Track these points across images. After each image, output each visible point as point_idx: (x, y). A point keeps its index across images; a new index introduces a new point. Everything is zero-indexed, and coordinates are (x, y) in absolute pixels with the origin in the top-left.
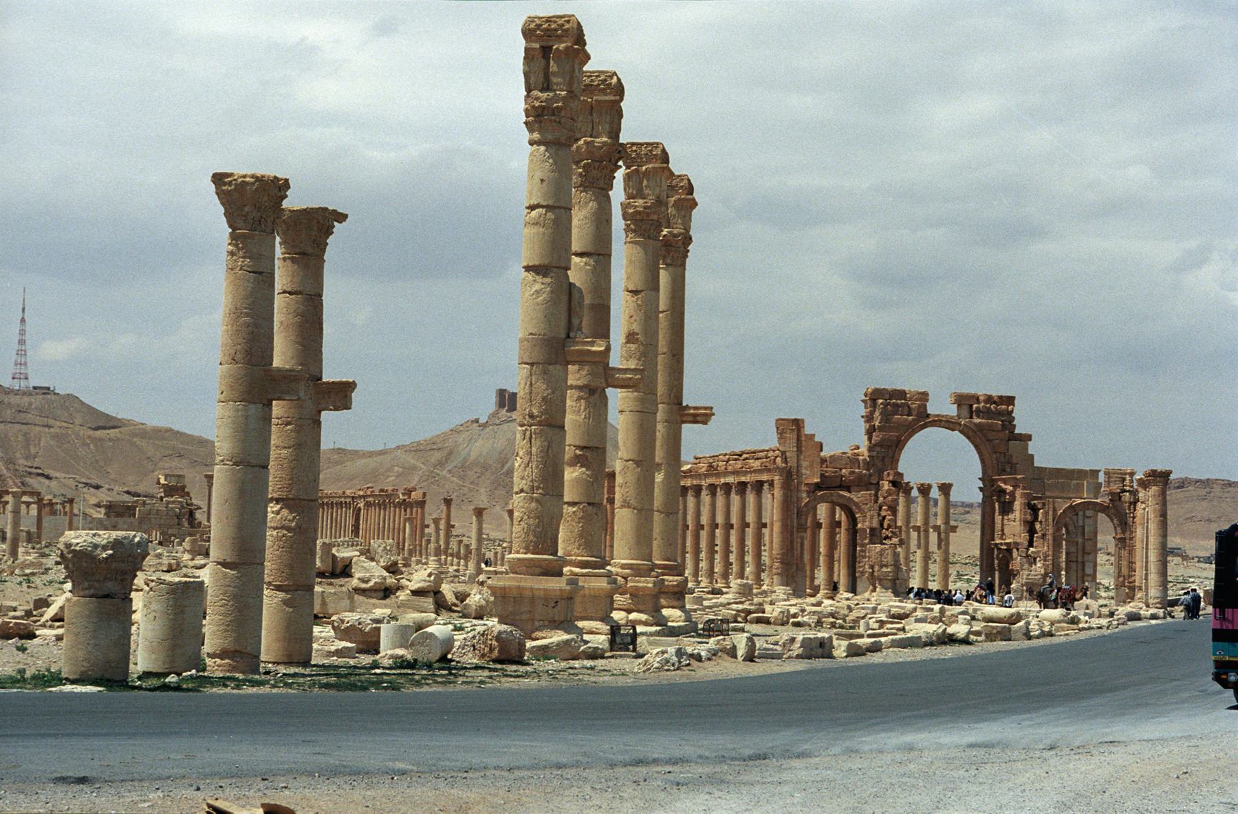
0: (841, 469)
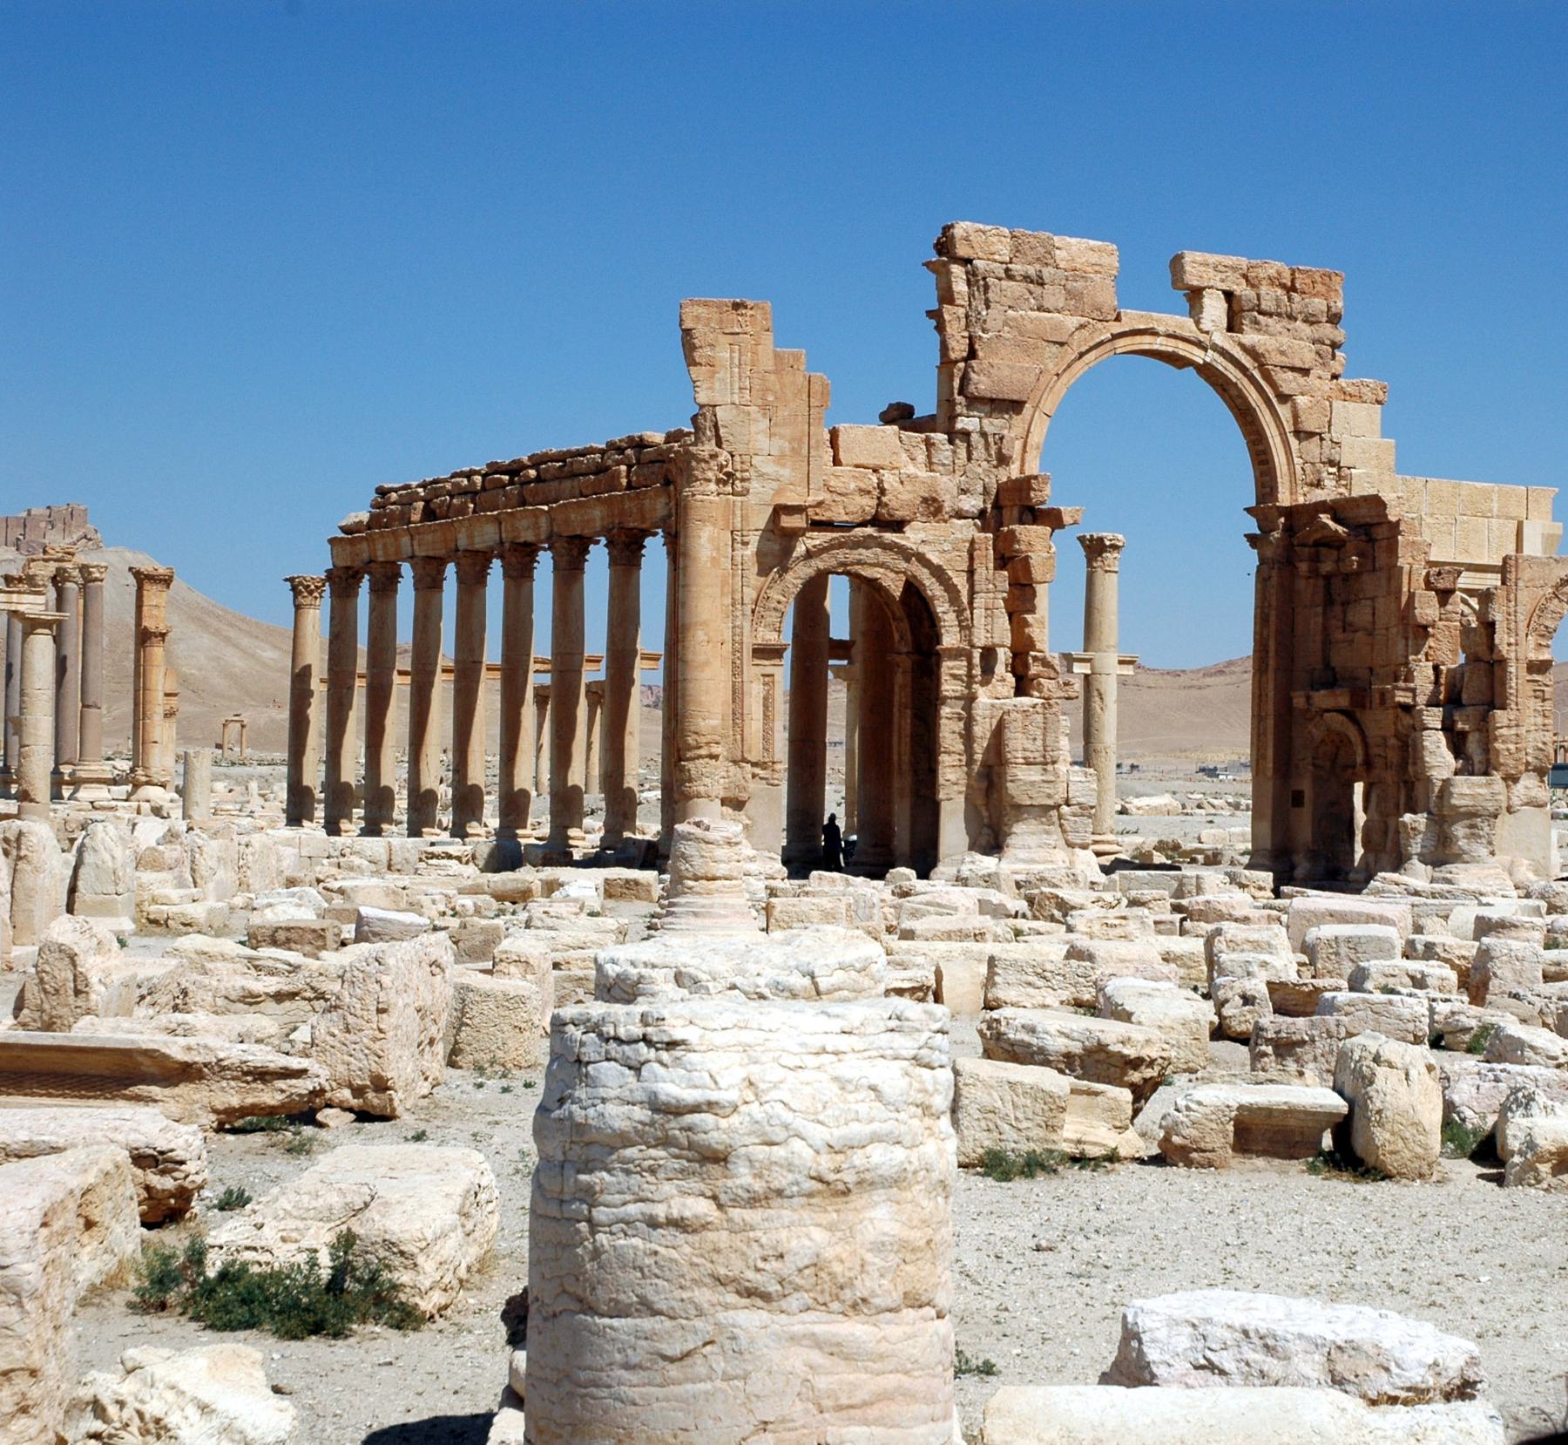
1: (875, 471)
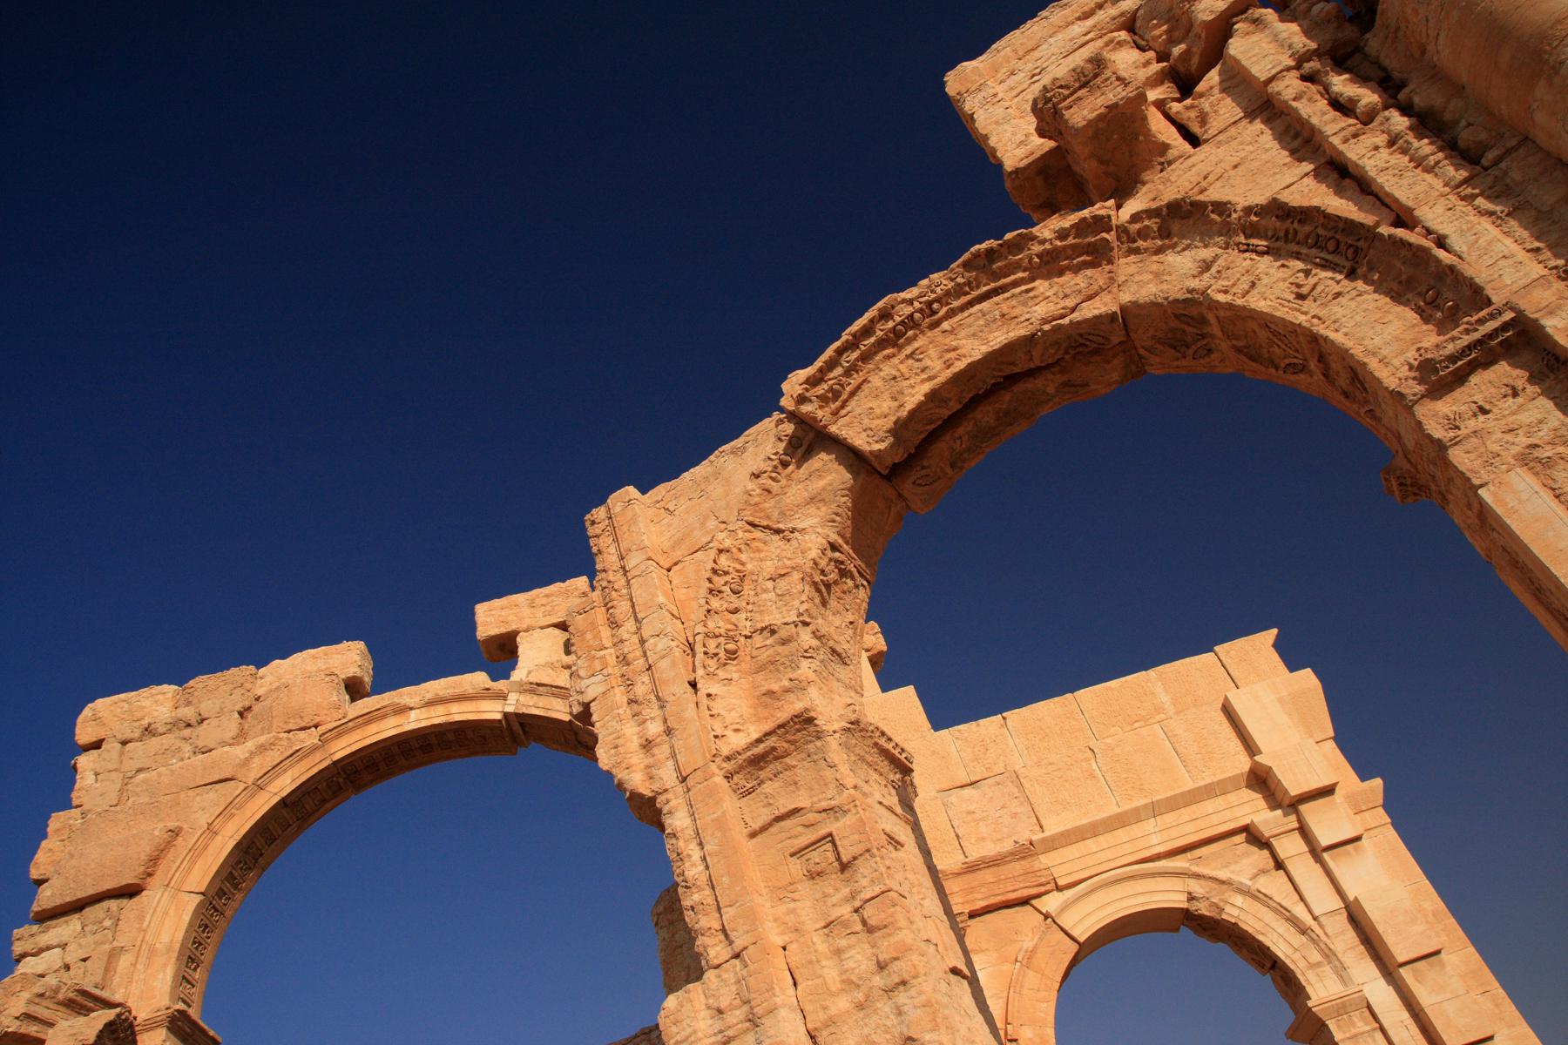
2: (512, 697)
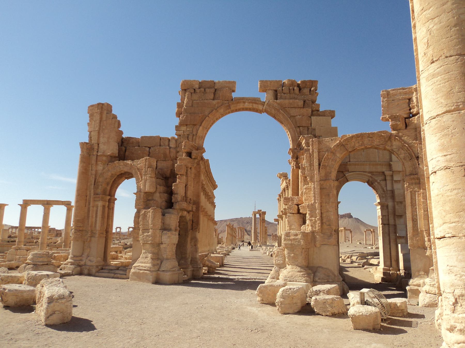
0: (150, 148)
1: (150, 148)
2: (265, 107)
